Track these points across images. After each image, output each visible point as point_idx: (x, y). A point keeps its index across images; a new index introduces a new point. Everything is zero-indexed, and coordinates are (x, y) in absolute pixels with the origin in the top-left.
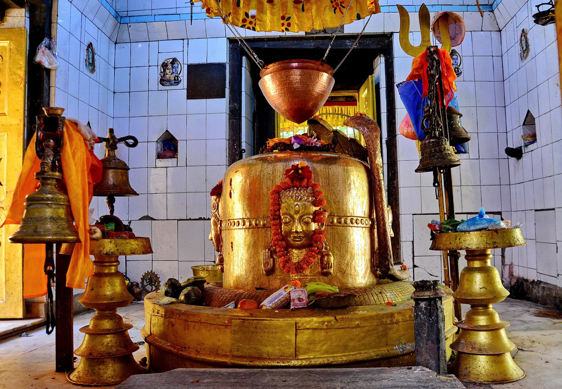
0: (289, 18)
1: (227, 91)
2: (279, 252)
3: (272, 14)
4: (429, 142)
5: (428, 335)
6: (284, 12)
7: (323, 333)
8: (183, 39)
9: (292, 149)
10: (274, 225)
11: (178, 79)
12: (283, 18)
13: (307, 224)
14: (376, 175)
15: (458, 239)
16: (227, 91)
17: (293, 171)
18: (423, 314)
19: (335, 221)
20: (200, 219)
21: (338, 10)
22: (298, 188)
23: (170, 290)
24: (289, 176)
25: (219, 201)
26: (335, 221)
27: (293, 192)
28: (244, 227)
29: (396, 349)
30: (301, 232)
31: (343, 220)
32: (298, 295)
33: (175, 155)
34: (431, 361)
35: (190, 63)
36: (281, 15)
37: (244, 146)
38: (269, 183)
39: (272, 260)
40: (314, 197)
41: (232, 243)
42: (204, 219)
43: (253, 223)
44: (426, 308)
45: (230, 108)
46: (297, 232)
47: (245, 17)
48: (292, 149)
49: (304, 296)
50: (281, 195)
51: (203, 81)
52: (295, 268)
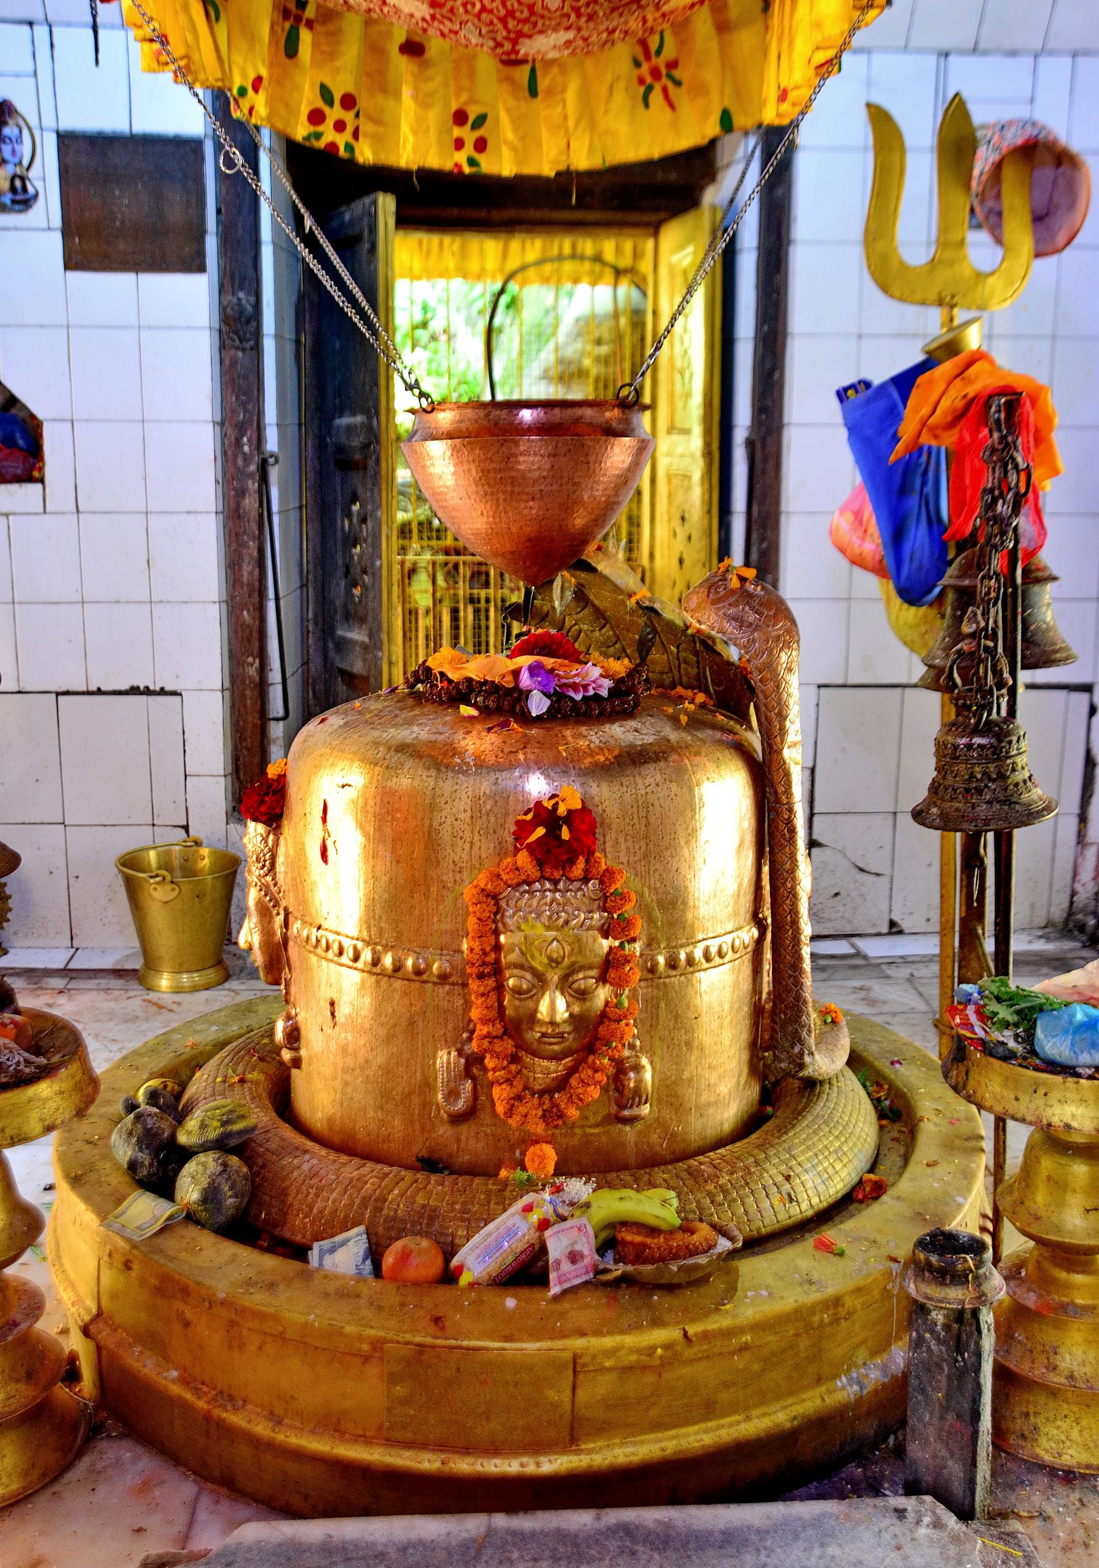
0: (481, 120)
1: (211, 243)
2: (494, 1070)
3: (423, 101)
4: (969, 746)
5: (948, 1397)
6: (464, 97)
7: (650, 1378)
8: (31, 24)
9: (526, 719)
10: (483, 995)
11: (25, 189)
12: (460, 118)
13: (583, 995)
14: (781, 789)
15: (1041, 1092)
16: (211, 243)
17: (541, 831)
18: (938, 1339)
19: (661, 960)
20: (134, 691)
21: (656, 96)
22: (555, 883)
23: (145, 1158)
24: (530, 848)
25: (276, 843)
26: (661, 960)
27: (544, 897)
28: (377, 970)
29: (843, 1388)
30: (565, 1022)
31: (683, 956)
32: (569, 1246)
33: (33, 467)
34: (950, 1463)
35: (66, 125)
36: (454, 107)
37: (272, 443)
38: (459, 850)
39: (469, 1085)
40: (604, 911)
41: (332, 1004)
42: (148, 692)
43: (409, 963)
44: (947, 1327)
45: (223, 309)
46: (553, 1023)
47: (320, 104)
48: (526, 719)
49: (586, 1247)
50: (503, 904)
51: (124, 204)
52: (544, 1116)
